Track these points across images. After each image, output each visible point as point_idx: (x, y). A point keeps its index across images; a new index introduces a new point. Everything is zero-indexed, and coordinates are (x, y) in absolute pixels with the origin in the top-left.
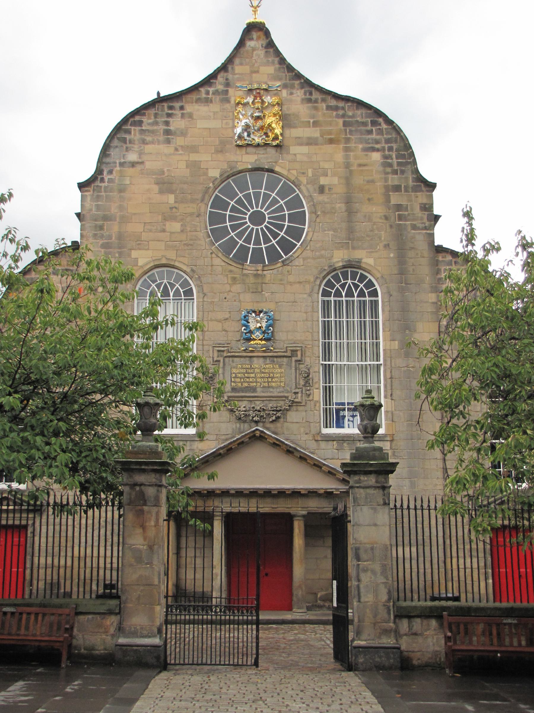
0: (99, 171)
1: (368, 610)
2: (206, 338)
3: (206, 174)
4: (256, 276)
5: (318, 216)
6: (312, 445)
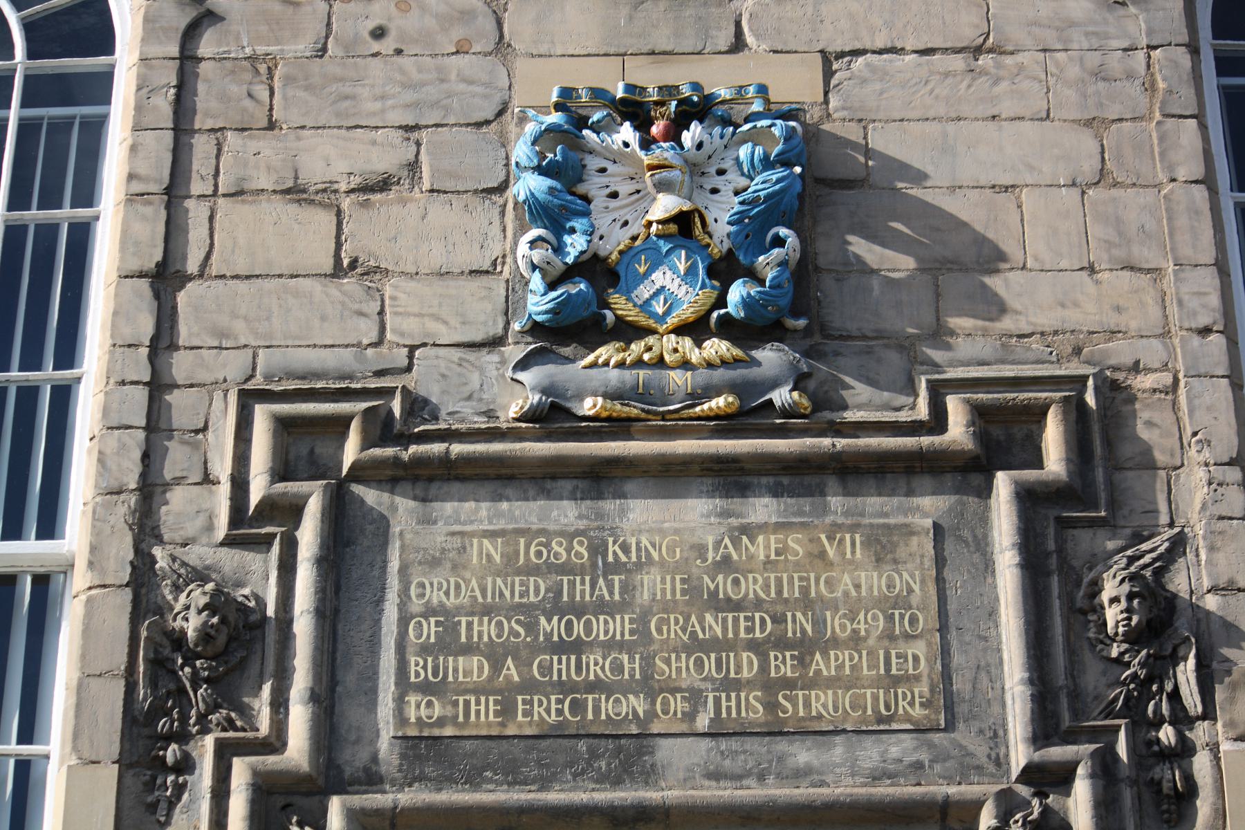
2: (186, 331)
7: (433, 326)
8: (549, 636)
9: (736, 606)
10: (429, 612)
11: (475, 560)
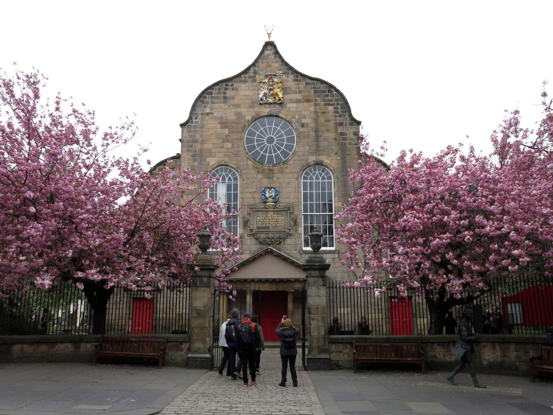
0: (190, 118)
1: (315, 340)
3: (244, 118)
4: (269, 170)
5: (301, 139)
6: (298, 256)
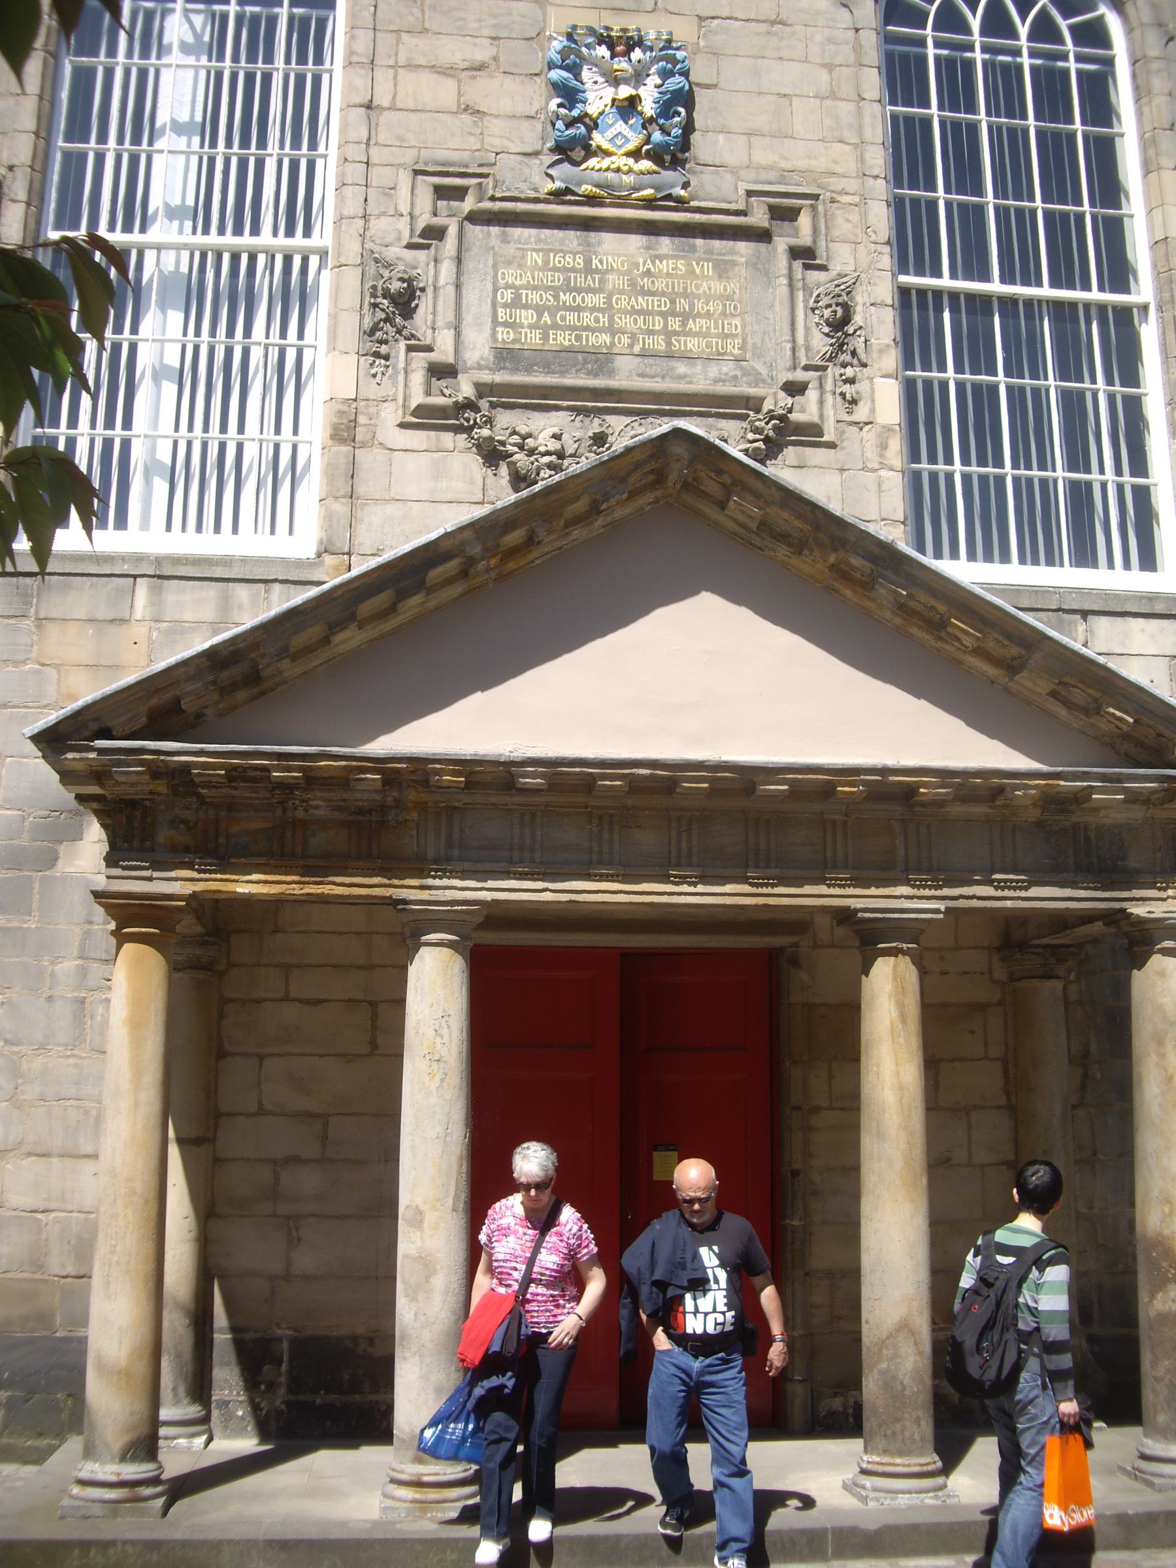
2: (382, 137)
7: (506, 143)
8: (564, 303)
9: (653, 294)
10: (507, 287)
11: (529, 263)
